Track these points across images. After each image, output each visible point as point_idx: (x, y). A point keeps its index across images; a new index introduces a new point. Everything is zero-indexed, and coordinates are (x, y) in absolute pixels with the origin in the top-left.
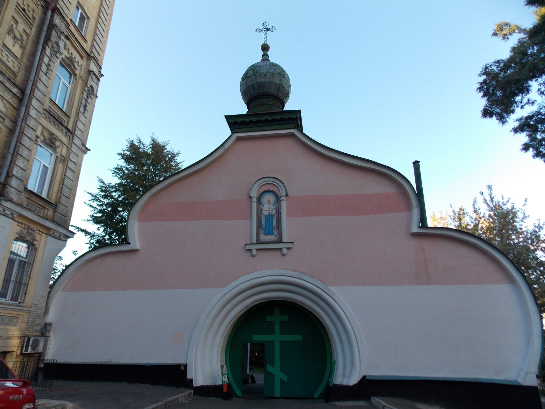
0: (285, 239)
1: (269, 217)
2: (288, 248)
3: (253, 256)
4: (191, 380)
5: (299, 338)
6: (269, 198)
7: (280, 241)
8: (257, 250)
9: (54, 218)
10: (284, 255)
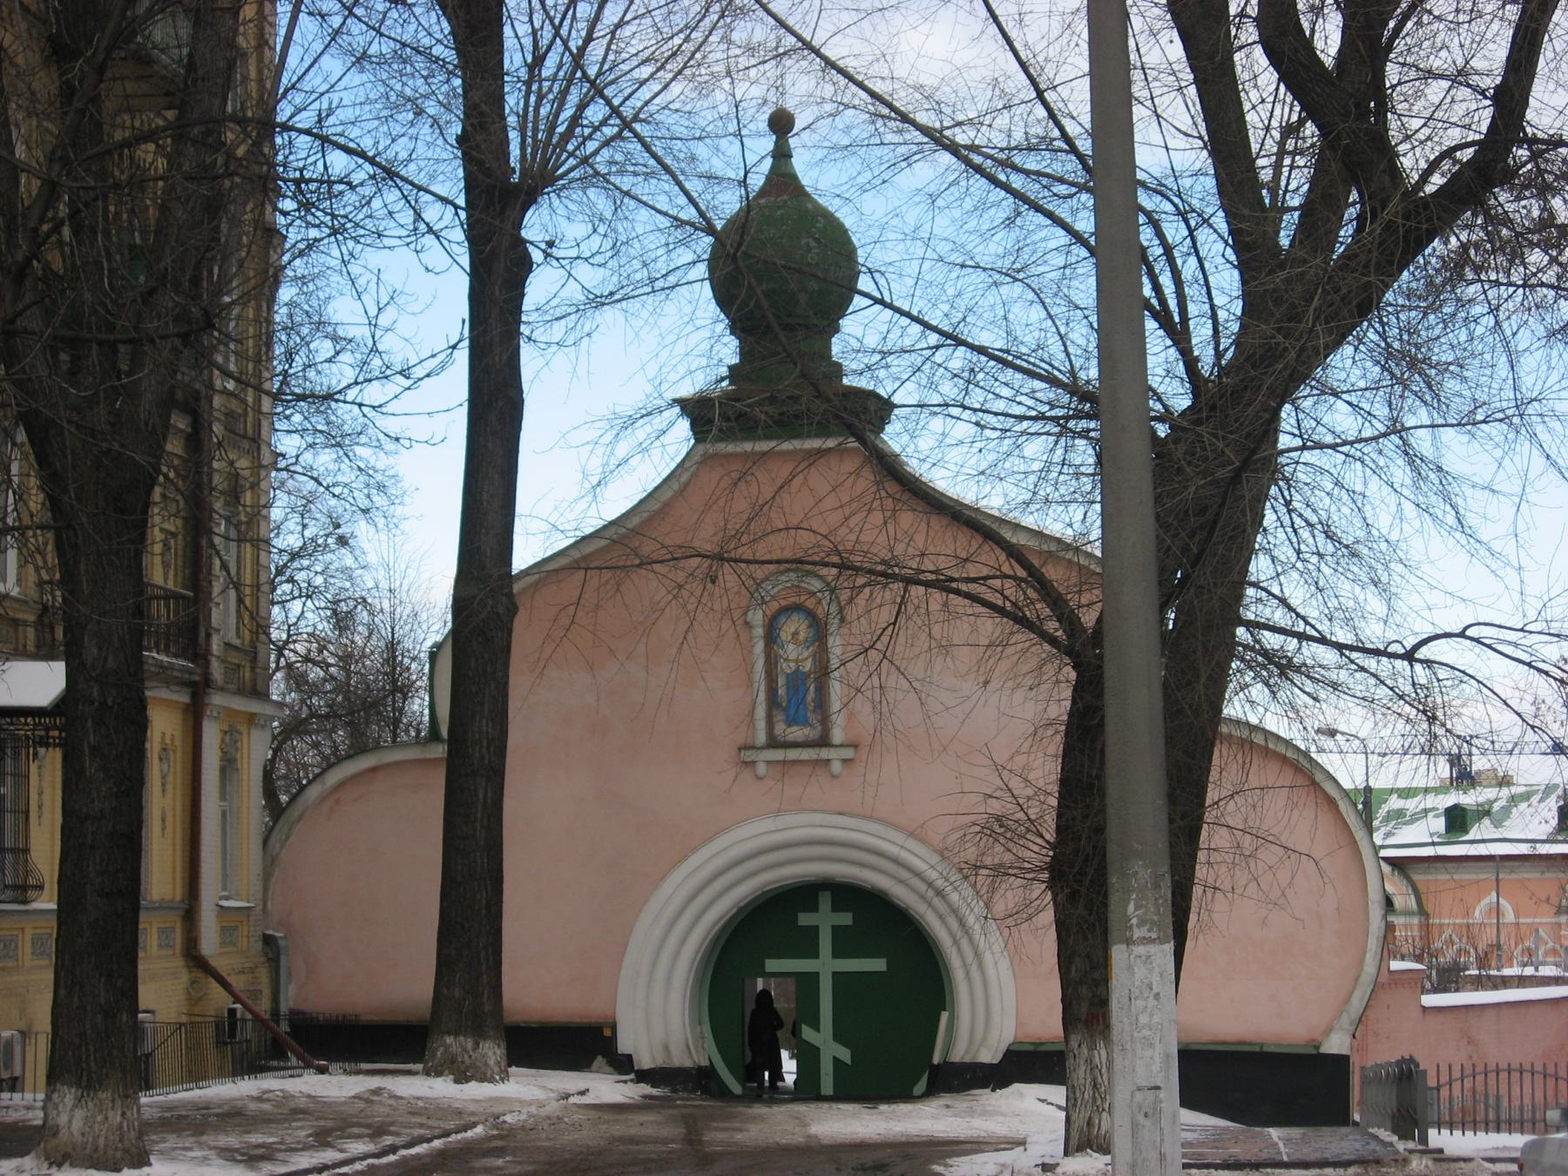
0: (837, 736)
1: (796, 680)
2: (845, 761)
3: (760, 778)
4: (629, 1057)
5: (878, 965)
6: (794, 626)
7: (824, 742)
8: (768, 762)
9: (255, 685)
10: (834, 777)
